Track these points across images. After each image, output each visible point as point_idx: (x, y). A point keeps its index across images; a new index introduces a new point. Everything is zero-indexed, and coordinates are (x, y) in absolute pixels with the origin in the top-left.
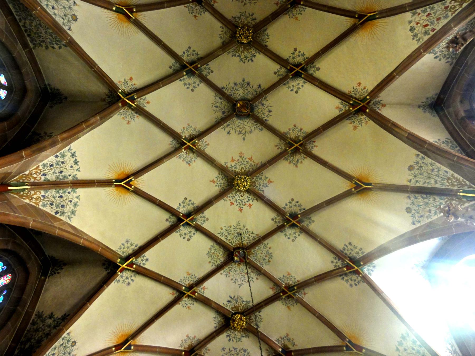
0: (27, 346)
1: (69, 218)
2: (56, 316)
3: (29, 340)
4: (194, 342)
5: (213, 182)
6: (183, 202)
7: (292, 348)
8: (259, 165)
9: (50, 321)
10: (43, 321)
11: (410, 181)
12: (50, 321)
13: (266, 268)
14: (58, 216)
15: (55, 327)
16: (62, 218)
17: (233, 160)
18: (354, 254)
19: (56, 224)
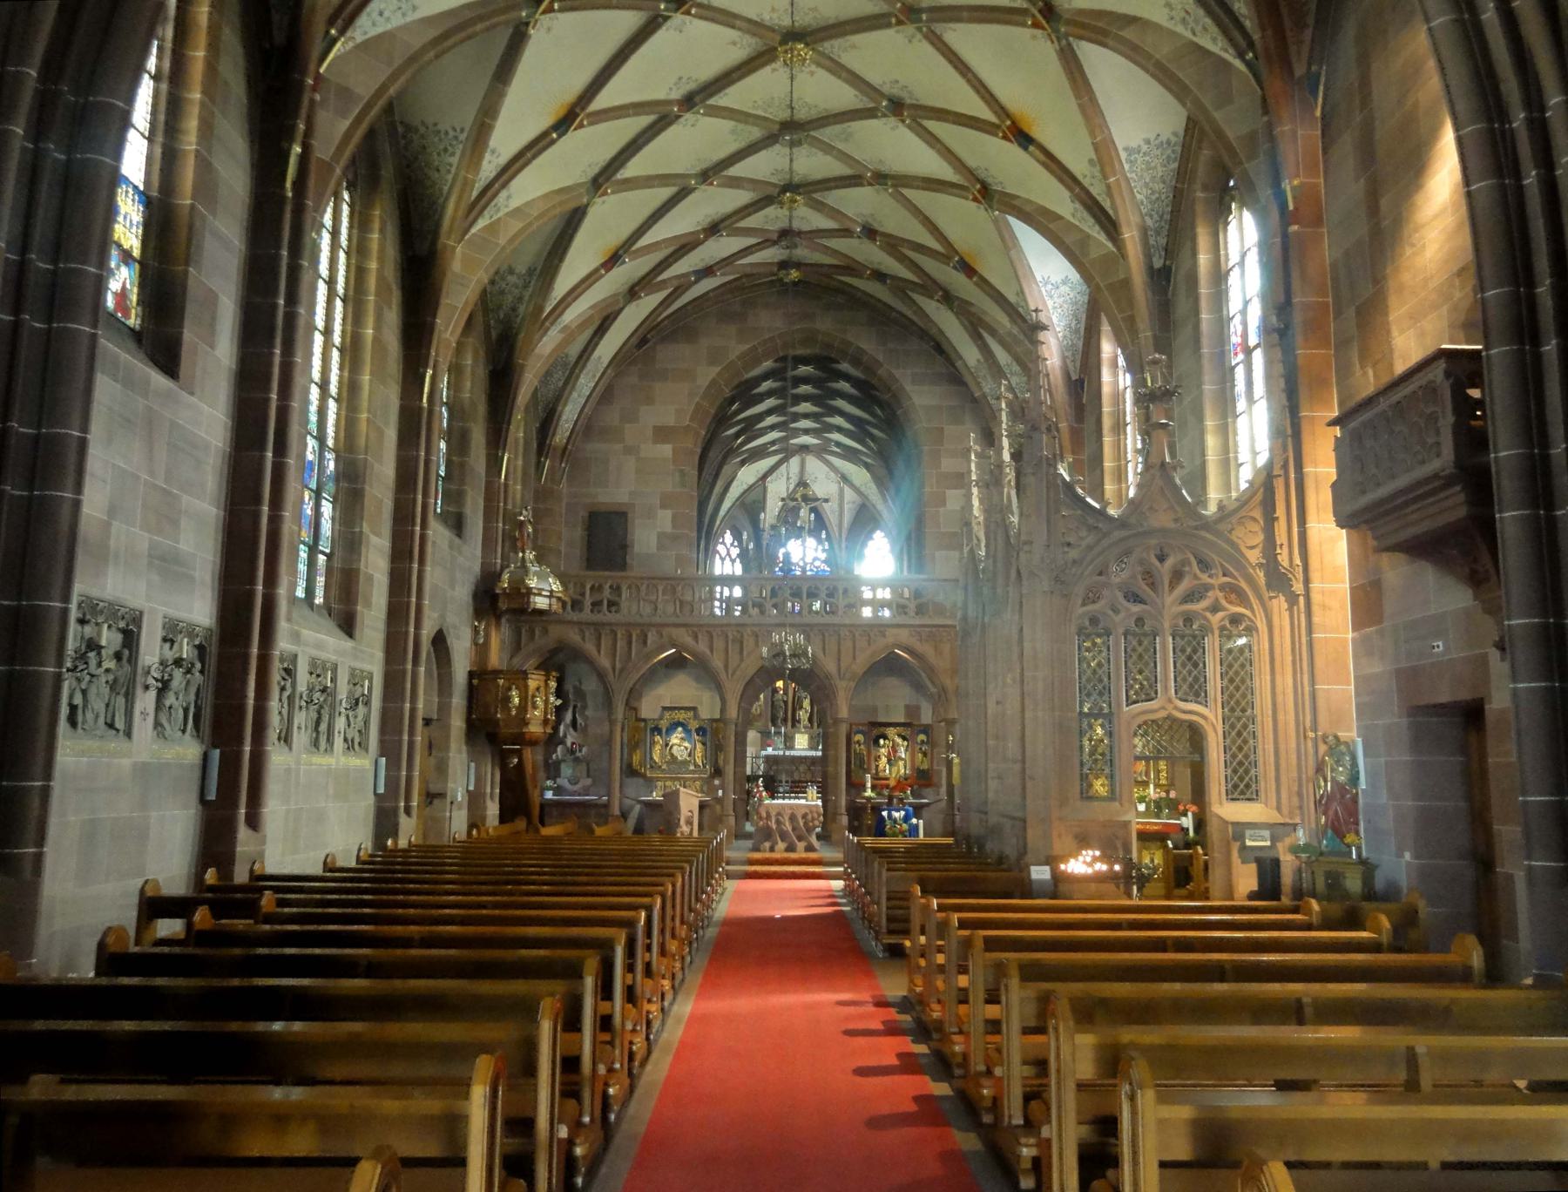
0: (502, 316)
1: (506, 206)
2: (517, 271)
3: (500, 307)
4: (716, 217)
5: (734, 43)
6: (675, 84)
7: (876, 226)
8: (831, 22)
9: (512, 279)
10: (503, 279)
11: (1085, 176)
12: (512, 279)
13: (840, 146)
14: (495, 218)
15: (526, 286)
16: (500, 215)
17: (773, 10)
18: (989, 180)
19: (502, 241)
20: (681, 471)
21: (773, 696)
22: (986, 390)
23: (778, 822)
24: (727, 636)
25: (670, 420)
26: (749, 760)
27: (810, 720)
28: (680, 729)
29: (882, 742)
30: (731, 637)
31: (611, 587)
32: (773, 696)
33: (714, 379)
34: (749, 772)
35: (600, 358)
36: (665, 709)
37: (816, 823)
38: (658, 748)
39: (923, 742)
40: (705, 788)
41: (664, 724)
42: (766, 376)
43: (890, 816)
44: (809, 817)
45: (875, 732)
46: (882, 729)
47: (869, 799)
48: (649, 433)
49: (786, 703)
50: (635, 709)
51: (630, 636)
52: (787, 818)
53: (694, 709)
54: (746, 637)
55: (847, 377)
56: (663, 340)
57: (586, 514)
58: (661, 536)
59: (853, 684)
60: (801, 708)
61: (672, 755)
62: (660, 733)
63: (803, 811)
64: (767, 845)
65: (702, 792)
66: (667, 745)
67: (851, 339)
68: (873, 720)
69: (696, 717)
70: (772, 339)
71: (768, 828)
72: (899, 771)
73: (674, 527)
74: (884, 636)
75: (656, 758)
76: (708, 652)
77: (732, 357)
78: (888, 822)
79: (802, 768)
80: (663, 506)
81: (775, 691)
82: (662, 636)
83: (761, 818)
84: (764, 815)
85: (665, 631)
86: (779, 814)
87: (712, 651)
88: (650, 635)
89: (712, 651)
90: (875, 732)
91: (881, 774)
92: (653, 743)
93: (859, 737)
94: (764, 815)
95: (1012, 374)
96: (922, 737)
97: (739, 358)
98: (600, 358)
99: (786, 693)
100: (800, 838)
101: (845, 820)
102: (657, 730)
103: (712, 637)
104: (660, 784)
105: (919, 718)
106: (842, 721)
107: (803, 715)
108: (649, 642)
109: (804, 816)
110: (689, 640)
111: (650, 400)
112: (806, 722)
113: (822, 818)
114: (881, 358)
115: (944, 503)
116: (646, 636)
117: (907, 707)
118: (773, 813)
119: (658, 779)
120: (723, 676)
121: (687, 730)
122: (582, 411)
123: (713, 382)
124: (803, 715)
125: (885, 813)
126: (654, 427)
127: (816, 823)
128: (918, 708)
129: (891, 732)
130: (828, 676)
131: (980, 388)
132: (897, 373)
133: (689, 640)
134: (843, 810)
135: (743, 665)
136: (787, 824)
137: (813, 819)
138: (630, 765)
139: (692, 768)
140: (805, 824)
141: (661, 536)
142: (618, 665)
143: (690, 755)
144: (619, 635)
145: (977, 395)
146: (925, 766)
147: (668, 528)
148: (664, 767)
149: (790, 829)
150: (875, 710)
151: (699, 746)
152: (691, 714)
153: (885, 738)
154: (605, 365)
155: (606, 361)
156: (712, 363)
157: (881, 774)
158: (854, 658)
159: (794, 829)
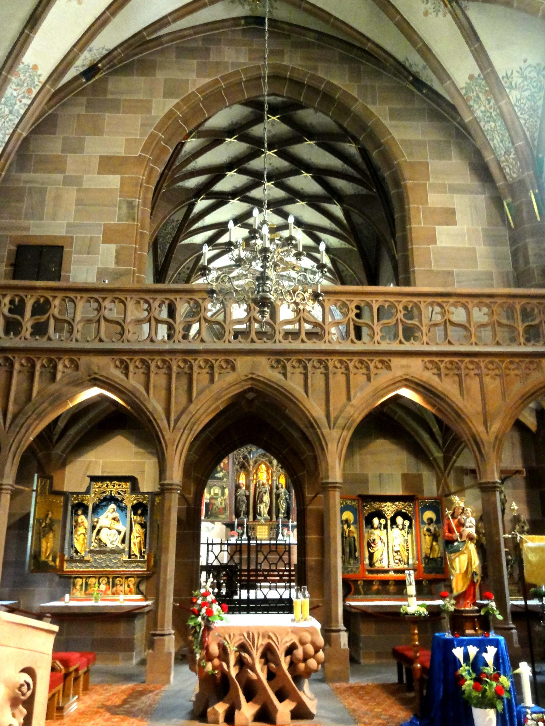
20: (130, 205)
21: (236, 491)
22: (479, 114)
23: (241, 663)
24: (170, 368)
25: (121, 151)
26: (203, 549)
27: (270, 512)
28: (113, 506)
29: (376, 521)
30: (175, 368)
31: (12, 302)
32: (236, 491)
33: (171, 111)
34: (203, 562)
35: (35, 67)
36: (94, 479)
37: (312, 663)
38: (81, 530)
39: (430, 521)
40: (143, 588)
41: (91, 500)
42: (229, 166)
43: (466, 656)
44: (299, 653)
45: (368, 509)
46: (376, 505)
47: (416, 619)
48: (96, 162)
49: (248, 497)
50: (51, 478)
51: (33, 366)
52: (257, 655)
53: (132, 480)
54: (195, 368)
55: (308, 167)
56: (116, 72)
57: (14, 248)
58: (101, 273)
59: (348, 435)
60: (262, 501)
61: (100, 541)
62: (85, 513)
63: (289, 640)
64: (221, 708)
65: (139, 592)
66: (94, 527)
67: (321, 74)
68: (365, 493)
69: (135, 489)
70: (237, 73)
71: (225, 676)
72: (470, 563)
73: (117, 263)
74: (389, 368)
75: (78, 545)
76: (142, 389)
77: (192, 89)
78: (464, 670)
79: (273, 557)
80: (106, 241)
81: (238, 487)
82: (77, 368)
83: (209, 658)
84: (215, 649)
85: (84, 360)
86: (242, 647)
87: (147, 389)
88: (60, 367)
89: (147, 389)
90: (368, 509)
91: (378, 565)
92: (76, 525)
93: (348, 515)
94: (215, 649)
95: (511, 88)
96: (429, 514)
97: (201, 90)
98: (35, 67)
99: (248, 487)
100: (281, 698)
101: (344, 638)
102: (82, 507)
103: (148, 367)
104: (79, 581)
105: (422, 491)
106: (334, 486)
107: (264, 509)
108: (59, 376)
109: (290, 651)
110: (117, 374)
111: (97, 130)
112: (266, 515)
113: (321, 654)
114: (355, 94)
115: (433, 240)
116: (55, 367)
117: (405, 477)
118: (232, 649)
119: (79, 575)
120: (163, 423)
121: (122, 509)
122: (14, 131)
123: (170, 114)
124: (264, 509)
125: (458, 652)
126: (101, 157)
127: (312, 663)
128: (420, 476)
129: (389, 509)
130: (312, 425)
131: (472, 113)
132: (373, 108)
133: (117, 374)
134: (341, 626)
135: (192, 408)
136: (258, 666)
137: (306, 658)
138: (36, 556)
139: (125, 558)
140: (292, 665)
141: (101, 273)
142: (11, 408)
143: (123, 541)
144: (17, 366)
145: (467, 119)
146: (436, 554)
147: (112, 265)
148: (88, 557)
149: (263, 677)
150: (364, 481)
151: (137, 528)
152: (126, 486)
153: (380, 515)
154: (43, 79)
155: (45, 72)
156: (169, 94)
157: (378, 565)
158: (349, 399)
159: (271, 676)
